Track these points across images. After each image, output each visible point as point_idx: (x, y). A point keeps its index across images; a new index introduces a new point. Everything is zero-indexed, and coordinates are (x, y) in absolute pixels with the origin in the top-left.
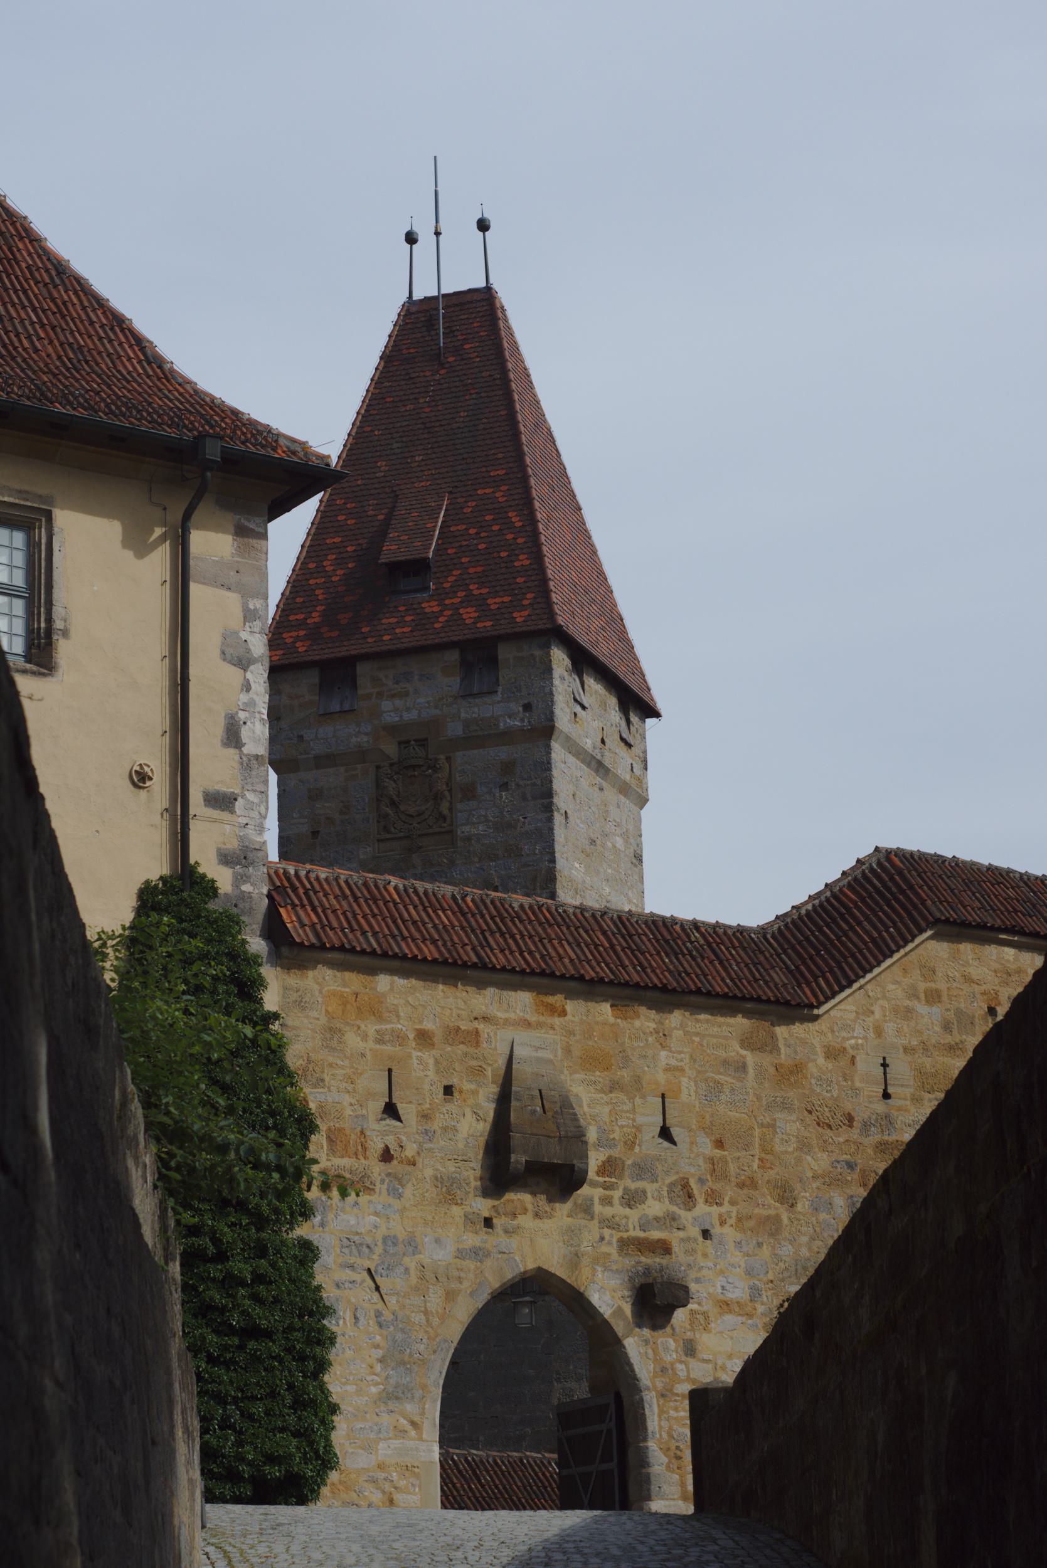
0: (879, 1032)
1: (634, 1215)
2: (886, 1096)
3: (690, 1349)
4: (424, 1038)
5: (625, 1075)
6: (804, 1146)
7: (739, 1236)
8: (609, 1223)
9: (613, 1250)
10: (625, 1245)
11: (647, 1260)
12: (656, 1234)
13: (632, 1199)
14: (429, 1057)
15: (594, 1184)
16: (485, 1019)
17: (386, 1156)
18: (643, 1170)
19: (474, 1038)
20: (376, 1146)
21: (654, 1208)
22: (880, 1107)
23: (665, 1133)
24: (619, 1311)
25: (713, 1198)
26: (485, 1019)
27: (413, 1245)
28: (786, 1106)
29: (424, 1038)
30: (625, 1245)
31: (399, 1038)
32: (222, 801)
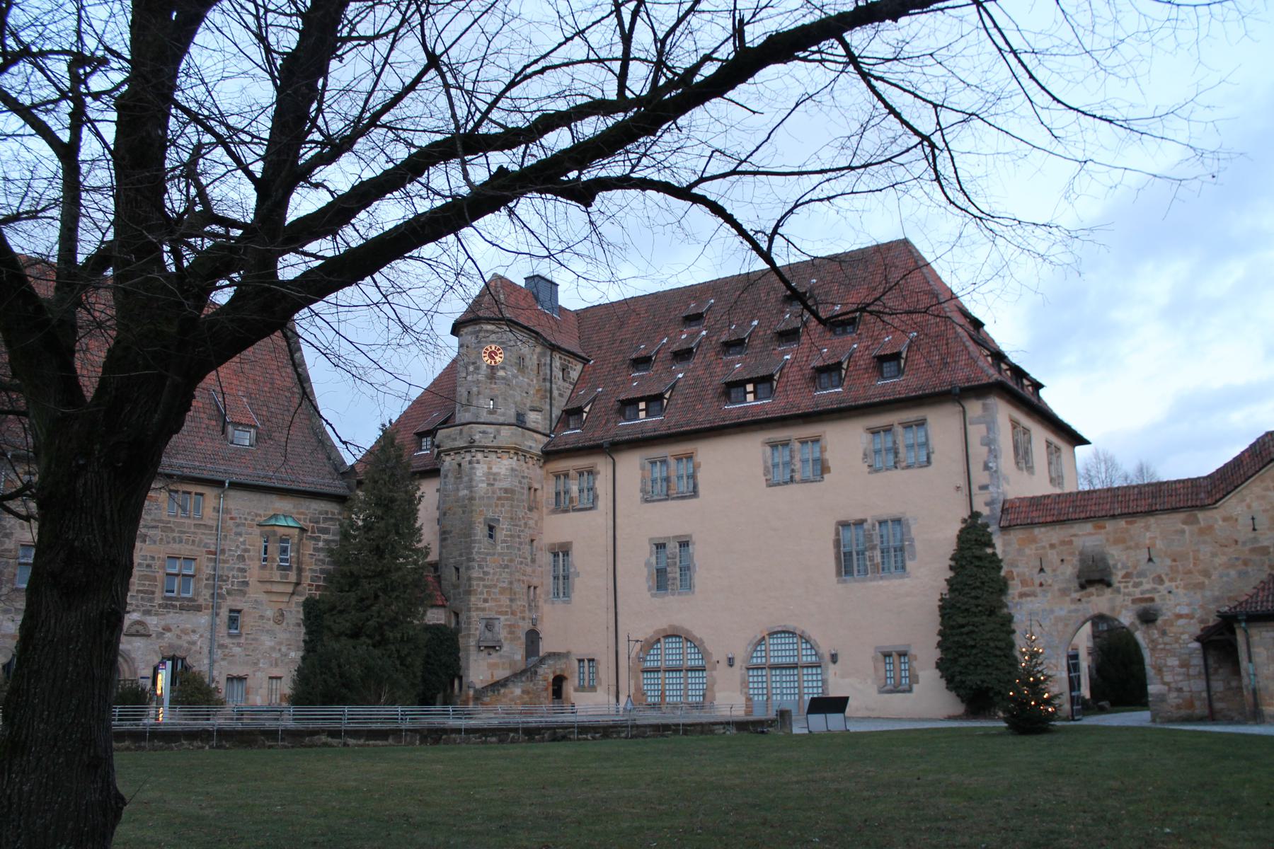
0: (1249, 507)
2: (1254, 529)
3: (1164, 633)
4: (1052, 546)
5: (1132, 544)
6: (1214, 555)
8: (1129, 594)
9: (1129, 603)
10: (1134, 601)
11: (1144, 605)
12: (1147, 596)
13: (1136, 585)
14: (1054, 551)
16: (1075, 535)
17: (1041, 585)
19: (1071, 542)
20: (1037, 582)
21: (1147, 586)
22: (1252, 535)
23: (1150, 560)
24: (1132, 624)
25: (1171, 580)
26: (1075, 535)
27: (1052, 611)
28: (1205, 542)
29: (1052, 546)
30: (1134, 601)
31: (1044, 548)
32: (984, 488)
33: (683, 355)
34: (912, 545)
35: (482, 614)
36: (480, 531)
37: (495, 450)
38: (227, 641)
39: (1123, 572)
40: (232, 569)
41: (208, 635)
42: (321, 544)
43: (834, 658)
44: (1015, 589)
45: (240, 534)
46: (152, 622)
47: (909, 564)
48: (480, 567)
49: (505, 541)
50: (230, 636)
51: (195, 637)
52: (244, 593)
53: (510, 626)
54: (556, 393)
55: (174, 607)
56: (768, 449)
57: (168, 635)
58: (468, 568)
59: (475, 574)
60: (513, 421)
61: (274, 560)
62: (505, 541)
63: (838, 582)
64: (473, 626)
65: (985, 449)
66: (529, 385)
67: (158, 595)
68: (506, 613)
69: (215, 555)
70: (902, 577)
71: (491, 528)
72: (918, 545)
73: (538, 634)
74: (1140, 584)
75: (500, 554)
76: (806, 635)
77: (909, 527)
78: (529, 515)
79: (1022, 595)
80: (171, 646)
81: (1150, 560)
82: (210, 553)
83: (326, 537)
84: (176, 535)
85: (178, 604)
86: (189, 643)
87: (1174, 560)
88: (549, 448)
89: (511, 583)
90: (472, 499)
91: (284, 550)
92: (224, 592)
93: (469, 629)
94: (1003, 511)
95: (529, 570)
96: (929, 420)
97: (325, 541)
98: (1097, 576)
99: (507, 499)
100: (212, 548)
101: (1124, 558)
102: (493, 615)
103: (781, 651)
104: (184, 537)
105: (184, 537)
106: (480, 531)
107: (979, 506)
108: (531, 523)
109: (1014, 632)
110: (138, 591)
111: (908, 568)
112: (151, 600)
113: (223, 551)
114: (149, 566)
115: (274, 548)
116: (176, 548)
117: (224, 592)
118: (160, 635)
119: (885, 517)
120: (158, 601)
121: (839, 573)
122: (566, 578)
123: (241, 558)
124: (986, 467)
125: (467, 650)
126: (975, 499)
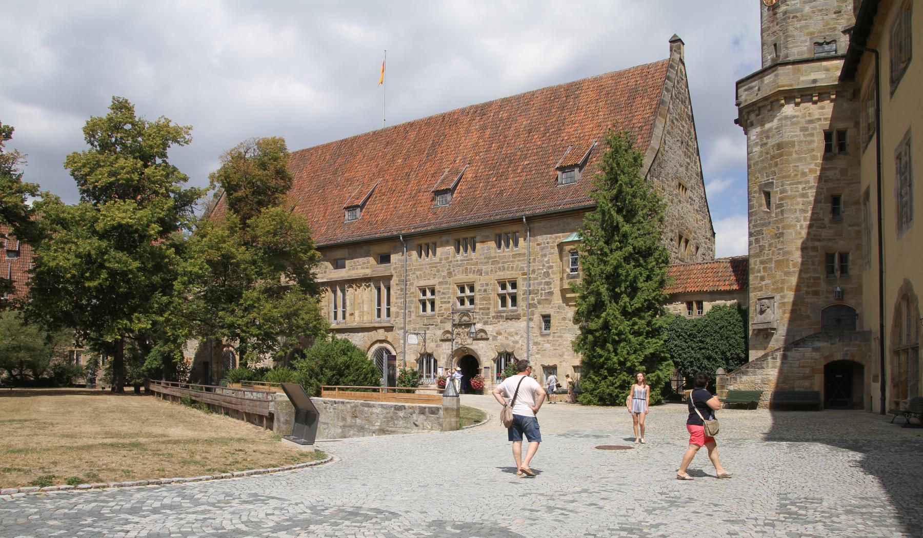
38: (540, 339)
40: (540, 284)
41: (525, 335)
45: (545, 256)
50: (542, 335)
51: (517, 338)
57: (500, 337)
71: (768, 195)
80: (502, 345)
84: (501, 265)
85: (504, 314)
86: (513, 342)
104: (506, 265)
105: (506, 265)
110: (480, 309)
112: (488, 314)
117: (536, 302)
118: (495, 338)
123: (547, 274)
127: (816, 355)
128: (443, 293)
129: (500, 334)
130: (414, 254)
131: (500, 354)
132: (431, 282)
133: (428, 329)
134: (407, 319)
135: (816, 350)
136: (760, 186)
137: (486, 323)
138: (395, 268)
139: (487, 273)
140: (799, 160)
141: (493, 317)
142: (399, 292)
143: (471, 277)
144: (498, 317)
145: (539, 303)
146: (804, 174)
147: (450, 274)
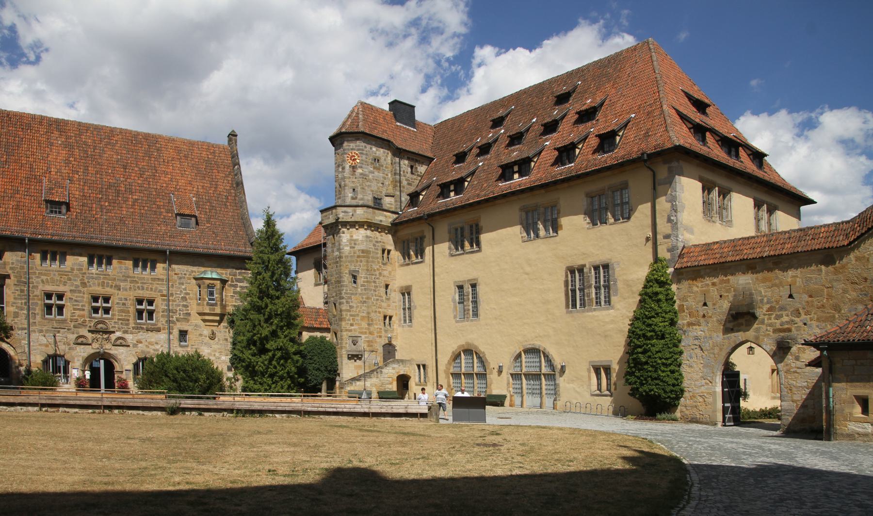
1: (778, 322)
5: (777, 281)
7: (818, 323)
8: (770, 325)
9: (771, 333)
12: (786, 326)
13: (778, 317)
14: (715, 289)
15: (765, 315)
17: (704, 316)
18: (782, 308)
21: (785, 319)
30: (775, 331)
32: (667, 237)
33: (484, 149)
34: (615, 284)
35: (350, 334)
36: (347, 279)
37: (353, 225)
39: (768, 306)
40: (179, 305)
42: (238, 289)
43: (563, 370)
44: (682, 321)
45: (183, 284)
46: (129, 337)
47: (613, 299)
48: (347, 302)
49: (362, 286)
52: (188, 321)
53: (368, 341)
54: (404, 183)
55: (142, 328)
56: (524, 214)
58: (340, 303)
59: (344, 307)
60: (371, 204)
61: (204, 300)
62: (362, 286)
63: (567, 312)
64: (344, 342)
65: (670, 204)
66: (385, 178)
67: (131, 321)
68: (365, 333)
69: (167, 297)
70: (608, 309)
71: (355, 277)
72: (620, 285)
73: (394, 347)
74: (781, 316)
75: (360, 294)
76: (546, 352)
77: (614, 269)
78: (383, 267)
79: (690, 324)
81: (791, 296)
82: (163, 296)
83: (241, 284)
87: (811, 296)
88: (397, 221)
89: (368, 313)
90: (340, 257)
91: (211, 294)
92: (174, 319)
93: (341, 343)
94: (679, 257)
95: (384, 304)
96: (631, 184)
97: (241, 287)
98: (745, 310)
99: (364, 257)
100: (165, 293)
101: (769, 294)
102: (357, 334)
103: (527, 364)
104: (145, 286)
105: (145, 286)
106: (347, 279)
107: (663, 253)
108: (385, 273)
109: (681, 353)
111: (612, 303)
112: (127, 325)
113: (172, 295)
114: (124, 304)
115: (205, 292)
116: (141, 294)
117: (174, 319)
119: (598, 263)
120: (132, 325)
121: (567, 306)
122: (409, 309)
124: (669, 220)
125: (341, 357)
126: (659, 248)
127: (393, 371)
128: (76, 301)
129: (141, 342)
130: (38, 256)
131: (140, 359)
132: (61, 289)
133: (59, 332)
134: (31, 321)
135: (394, 368)
136: (350, 271)
137: (125, 332)
138: (11, 268)
139: (126, 290)
140: (373, 262)
141: (133, 328)
142: (18, 293)
143: (108, 291)
144: (138, 328)
145: (178, 320)
146: (375, 270)
147: (84, 284)
